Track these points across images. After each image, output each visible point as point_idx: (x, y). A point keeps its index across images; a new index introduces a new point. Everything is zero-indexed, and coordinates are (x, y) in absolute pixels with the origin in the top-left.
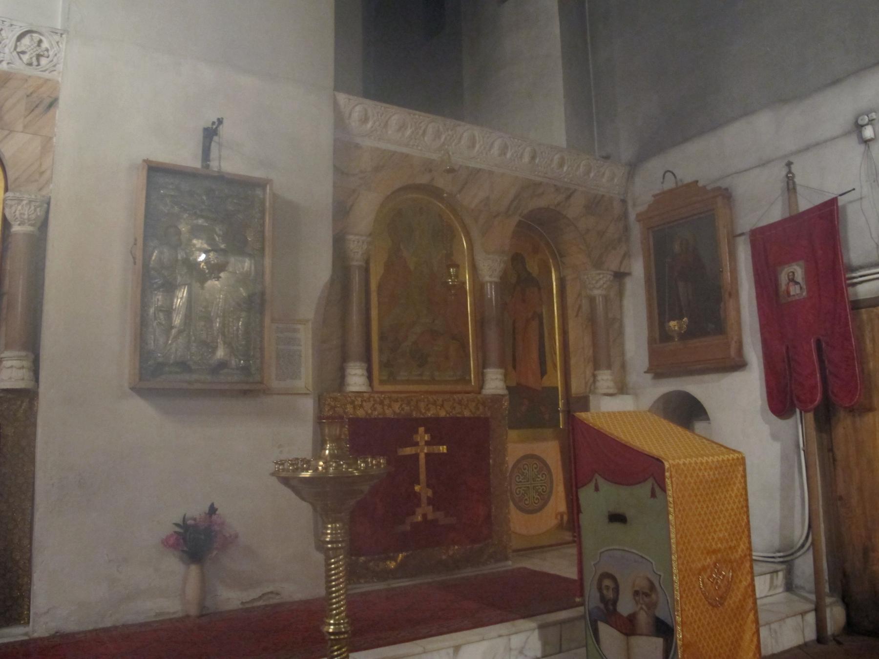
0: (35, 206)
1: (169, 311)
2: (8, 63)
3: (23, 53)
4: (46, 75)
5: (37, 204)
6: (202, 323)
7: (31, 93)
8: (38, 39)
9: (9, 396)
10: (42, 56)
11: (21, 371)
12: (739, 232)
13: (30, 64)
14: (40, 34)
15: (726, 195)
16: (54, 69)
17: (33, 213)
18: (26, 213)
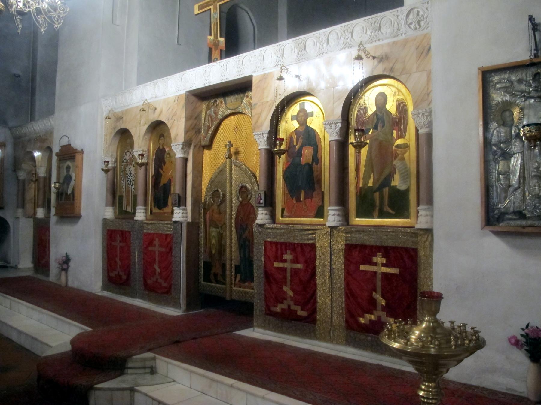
0: (426, 116)
1: (507, 174)
2: (405, 34)
3: (411, 24)
4: (425, 31)
5: (427, 114)
6: (535, 181)
7: (418, 47)
8: (416, 12)
9: (421, 233)
10: (421, 21)
11: (426, 217)
13: (416, 29)
14: (417, 8)
16: (428, 26)
17: (426, 120)
18: (422, 121)
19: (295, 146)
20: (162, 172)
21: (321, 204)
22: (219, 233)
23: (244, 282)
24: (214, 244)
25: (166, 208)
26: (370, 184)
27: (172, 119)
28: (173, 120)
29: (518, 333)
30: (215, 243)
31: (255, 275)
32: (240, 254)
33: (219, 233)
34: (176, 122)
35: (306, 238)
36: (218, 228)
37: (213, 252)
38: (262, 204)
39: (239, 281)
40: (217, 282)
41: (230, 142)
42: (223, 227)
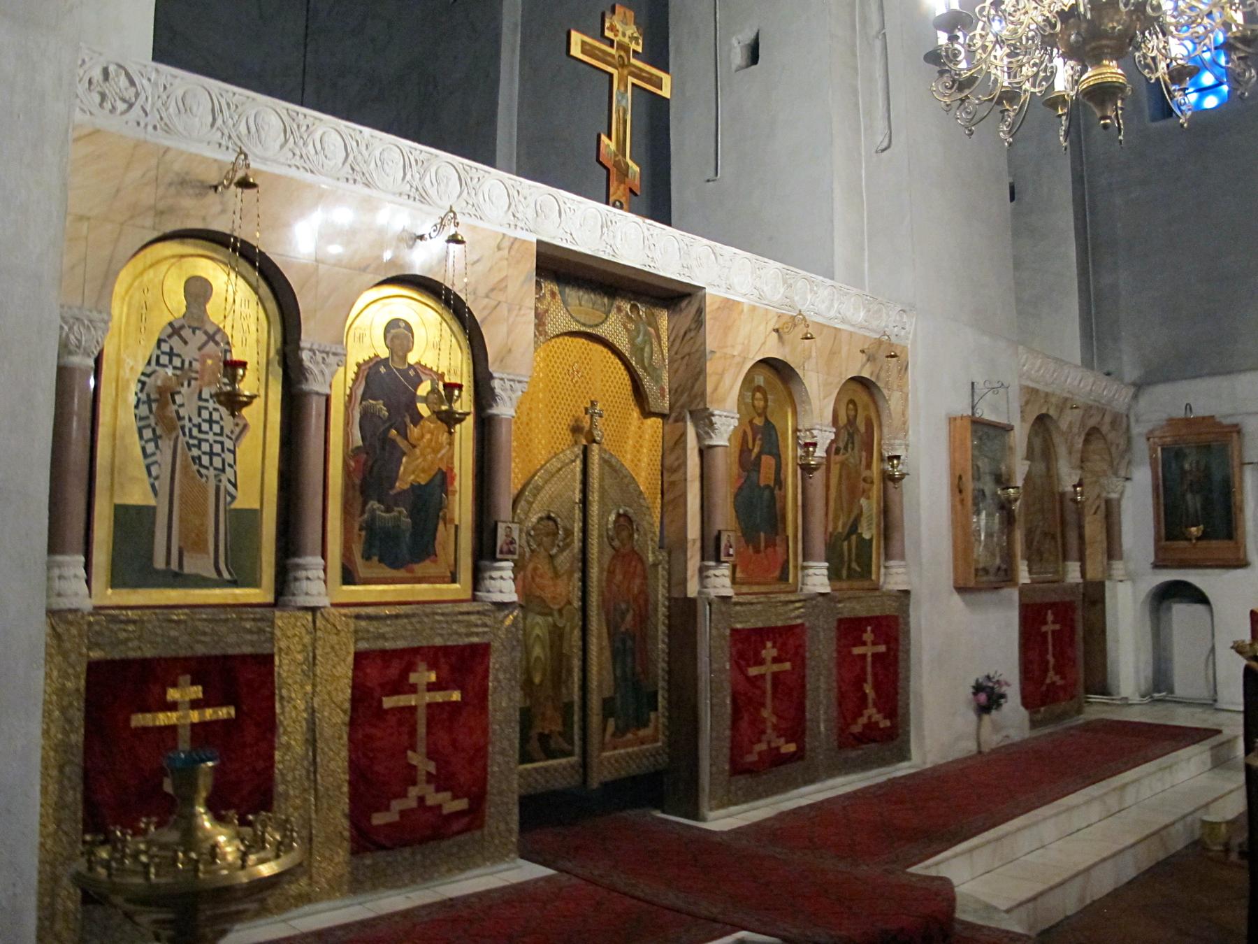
12: (1247, 460)
15: (1237, 429)
19: (751, 451)
20: (402, 443)
21: (785, 557)
22: (555, 625)
23: (623, 734)
24: (538, 658)
25: (427, 563)
26: (840, 530)
27: (487, 296)
28: (494, 303)
29: (1231, 645)
30: (542, 656)
31: (728, 701)
32: (614, 670)
33: (555, 625)
34: (504, 309)
35: (793, 615)
36: (551, 614)
37: (537, 680)
38: (731, 555)
39: (614, 735)
40: (550, 755)
41: (593, 404)
42: (564, 612)
